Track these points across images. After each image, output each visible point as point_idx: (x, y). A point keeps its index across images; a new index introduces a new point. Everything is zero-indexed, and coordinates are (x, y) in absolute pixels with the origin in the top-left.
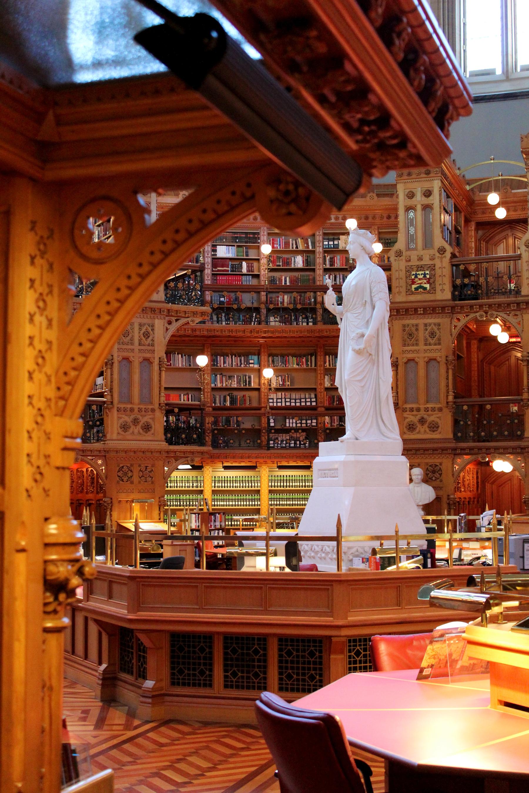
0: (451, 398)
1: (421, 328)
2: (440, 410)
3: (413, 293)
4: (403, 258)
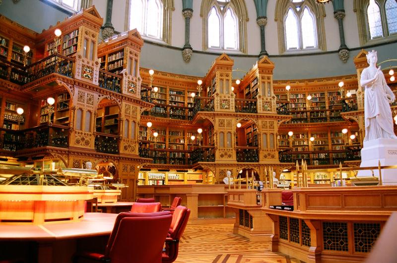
0: (95, 131)
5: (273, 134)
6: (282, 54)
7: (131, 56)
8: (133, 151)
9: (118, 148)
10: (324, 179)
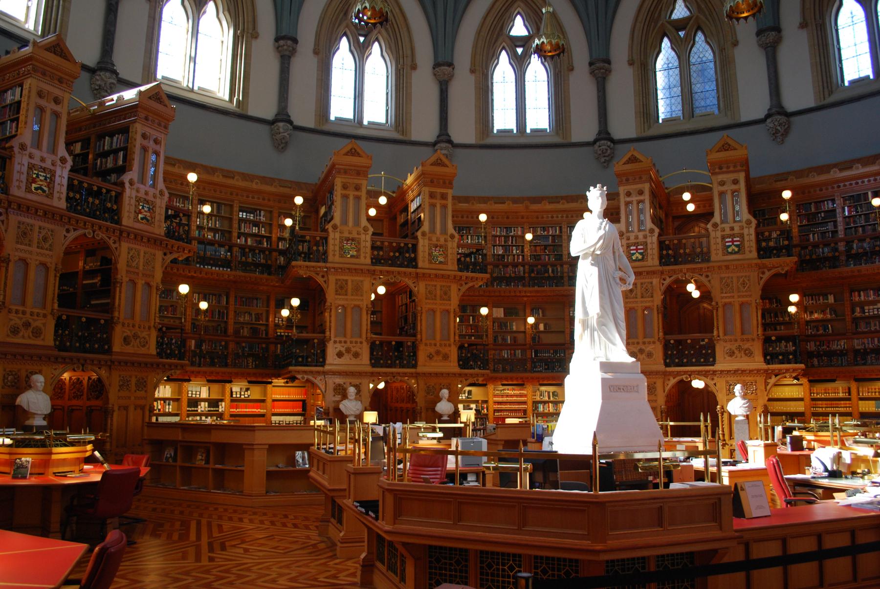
0: (56, 306)
1: (37, 229)
2: (45, 316)
3: (30, 191)
4: (27, 153)
5: (448, 311)
6: (482, 142)
7: (145, 143)
8: (144, 346)
9: (109, 341)
10: (552, 399)
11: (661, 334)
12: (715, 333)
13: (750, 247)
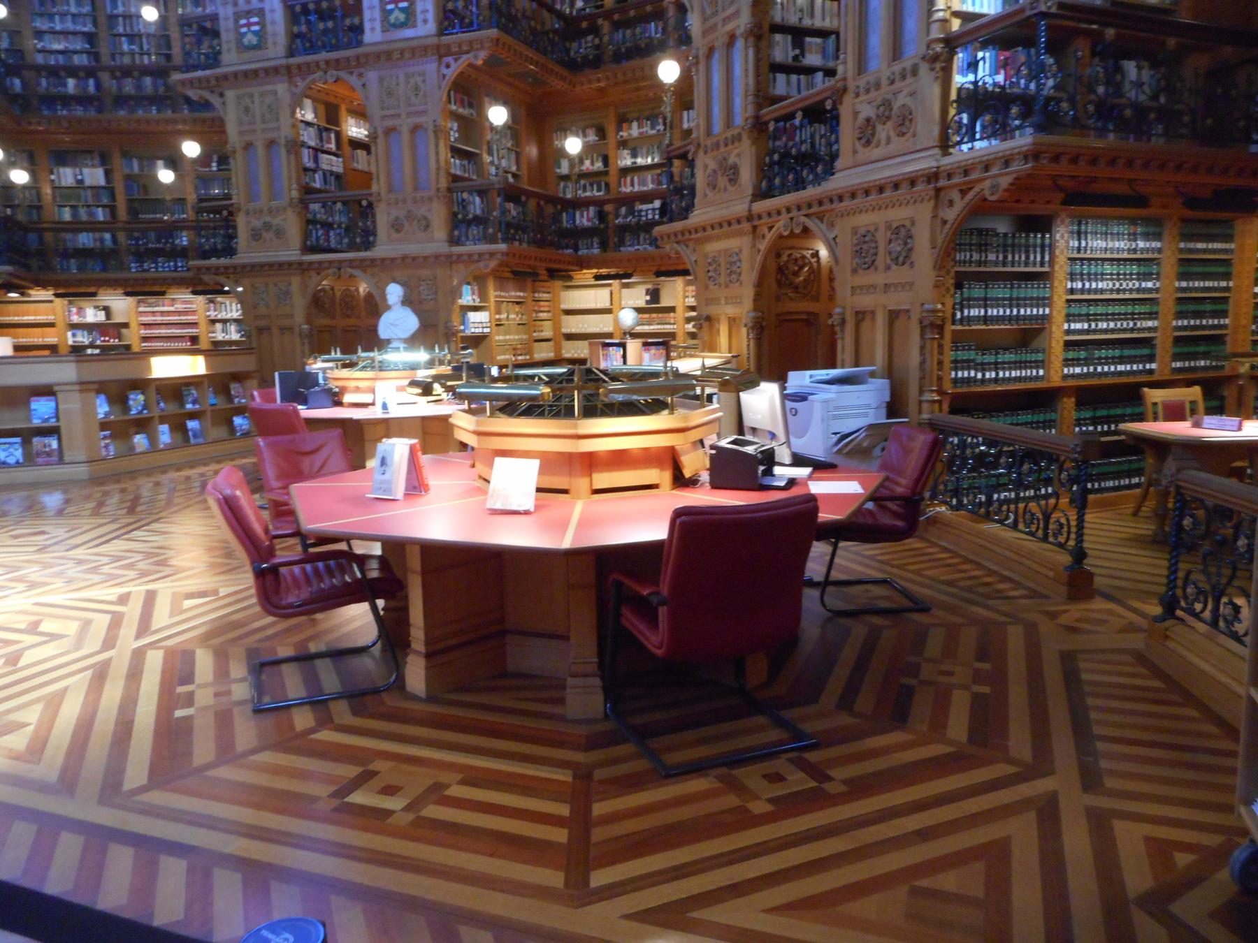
11: (295, 194)
12: (374, 188)
13: (425, 11)
